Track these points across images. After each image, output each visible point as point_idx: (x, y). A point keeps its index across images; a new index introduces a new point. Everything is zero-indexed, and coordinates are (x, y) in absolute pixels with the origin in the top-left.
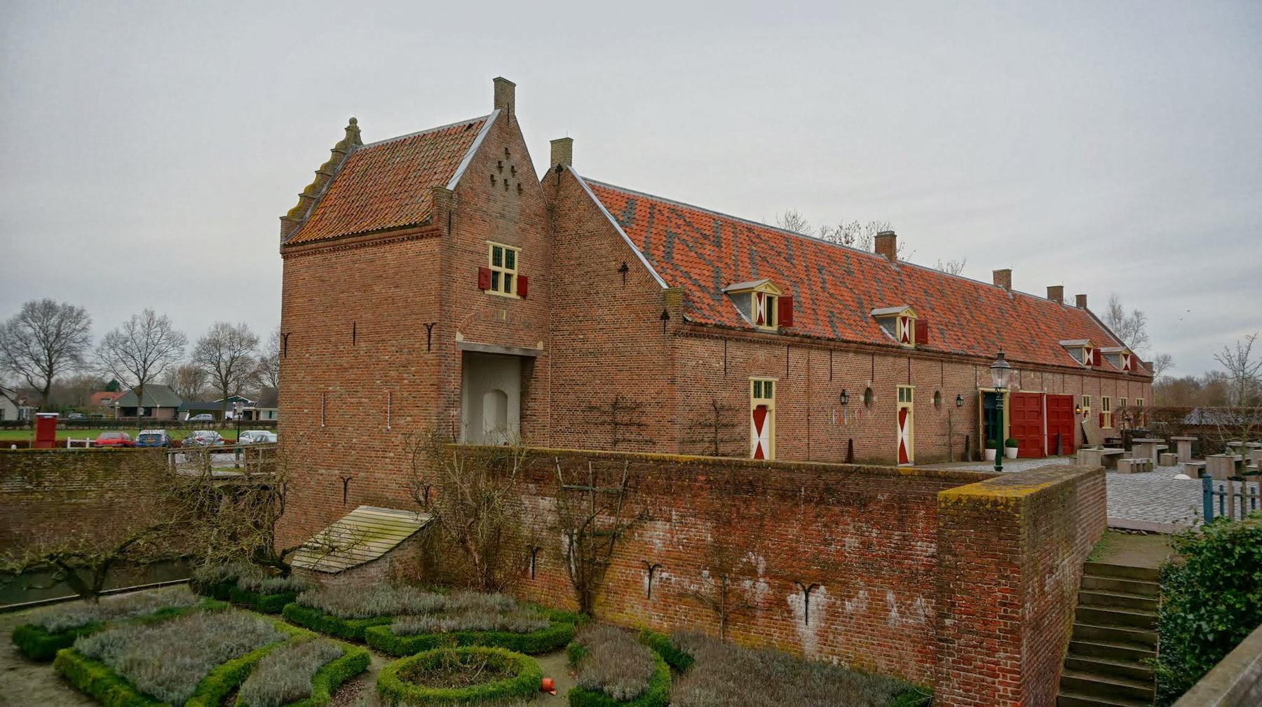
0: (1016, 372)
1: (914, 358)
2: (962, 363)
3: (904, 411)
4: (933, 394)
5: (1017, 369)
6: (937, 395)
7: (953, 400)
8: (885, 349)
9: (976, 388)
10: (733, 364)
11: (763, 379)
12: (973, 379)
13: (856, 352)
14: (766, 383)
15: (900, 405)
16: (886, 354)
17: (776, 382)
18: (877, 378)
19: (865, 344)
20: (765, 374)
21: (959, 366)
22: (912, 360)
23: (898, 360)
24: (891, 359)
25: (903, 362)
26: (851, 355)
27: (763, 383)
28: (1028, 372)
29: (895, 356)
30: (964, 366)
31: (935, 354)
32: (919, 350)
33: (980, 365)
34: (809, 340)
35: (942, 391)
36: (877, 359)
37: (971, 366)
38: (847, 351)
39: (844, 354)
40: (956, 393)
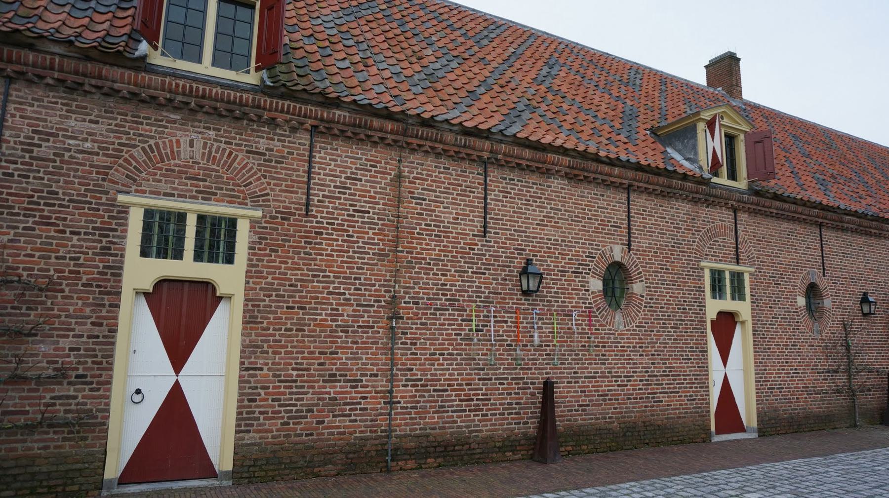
1: (750, 212)
6: (812, 291)
7: (853, 303)
8: (661, 180)
10: (45, 150)
11: (193, 209)
13: (572, 177)
14: (201, 218)
15: (713, 307)
16: (666, 194)
17: (254, 222)
18: (642, 242)
19: (597, 159)
20: (207, 196)
21: (861, 240)
23: (704, 212)
24: (683, 208)
25: (722, 217)
26: (556, 183)
27: (191, 222)
29: (695, 201)
30: (872, 241)
31: (800, 209)
32: (757, 193)
34: (389, 126)
35: (823, 283)
36: (639, 202)
38: (546, 173)
39: (534, 178)
40: (858, 290)
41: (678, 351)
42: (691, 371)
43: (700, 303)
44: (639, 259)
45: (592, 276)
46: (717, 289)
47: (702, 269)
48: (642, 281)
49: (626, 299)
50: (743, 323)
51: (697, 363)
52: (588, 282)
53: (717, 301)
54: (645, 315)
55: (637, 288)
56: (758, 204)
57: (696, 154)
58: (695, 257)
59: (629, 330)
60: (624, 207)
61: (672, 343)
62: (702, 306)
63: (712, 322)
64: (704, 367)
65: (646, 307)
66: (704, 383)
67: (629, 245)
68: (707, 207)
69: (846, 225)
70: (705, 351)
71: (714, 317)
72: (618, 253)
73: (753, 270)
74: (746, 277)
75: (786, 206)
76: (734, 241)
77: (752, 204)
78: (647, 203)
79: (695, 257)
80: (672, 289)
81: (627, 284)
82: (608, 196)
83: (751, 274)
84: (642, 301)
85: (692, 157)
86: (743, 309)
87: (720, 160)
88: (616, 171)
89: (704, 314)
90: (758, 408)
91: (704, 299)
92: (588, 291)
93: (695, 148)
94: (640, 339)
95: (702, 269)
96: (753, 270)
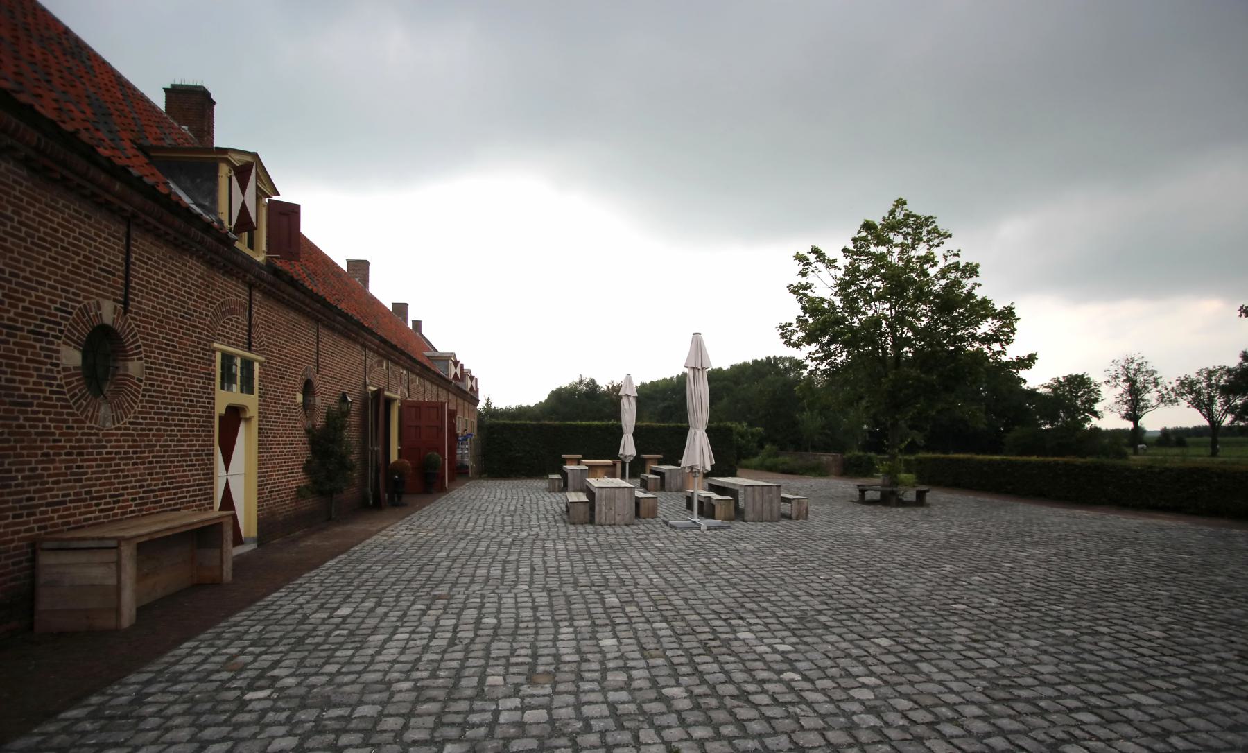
0: (405, 372)
1: (267, 294)
2: (348, 337)
3: (234, 415)
4: (299, 385)
5: (407, 369)
6: (308, 388)
9: (365, 385)
12: (361, 369)
15: (223, 399)
18: (144, 303)
21: (343, 342)
22: (257, 296)
23: (220, 280)
25: (236, 292)
28: (414, 376)
29: (211, 264)
31: (308, 301)
32: (277, 272)
33: (370, 349)
35: (317, 381)
36: (143, 245)
37: (359, 348)
41: (182, 456)
42: (195, 480)
43: (209, 394)
44: (138, 326)
45: (65, 343)
46: (228, 378)
47: (214, 351)
48: (140, 359)
49: (112, 383)
50: (248, 420)
51: (202, 470)
52: (57, 352)
53: (225, 392)
54: (142, 407)
55: (134, 368)
56: (273, 286)
57: (215, 201)
58: (207, 336)
59: (118, 429)
60: (120, 247)
61: (175, 446)
62: (211, 398)
63: (221, 418)
64: (209, 475)
65: (144, 396)
66: (209, 494)
67: (126, 303)
68: (223, 275)
69: (337, 325)
70: (211, 454)
71: (223, 412)
72: (108, 312)
73: (262, 359)
74: (256, 365)
75: (297, 294)
76: (246, 323)
77: (269, 283)
78: (154, 249)
79: (207, 336)
80: (178, 374)
81: (115, 360)
82: (97, 221)
83: (261, 364)
84: (140, 387)
85: (207, 204)
86: (251, 403)
87: (254, 221)
88: (118, 186)
89: (213, 408)
90: (258, 515)
91: (213, 389)
92: (57, 365)
93: (213, 194)
94: (134, 441)
95: (214, 351)
96: (262, 359)
